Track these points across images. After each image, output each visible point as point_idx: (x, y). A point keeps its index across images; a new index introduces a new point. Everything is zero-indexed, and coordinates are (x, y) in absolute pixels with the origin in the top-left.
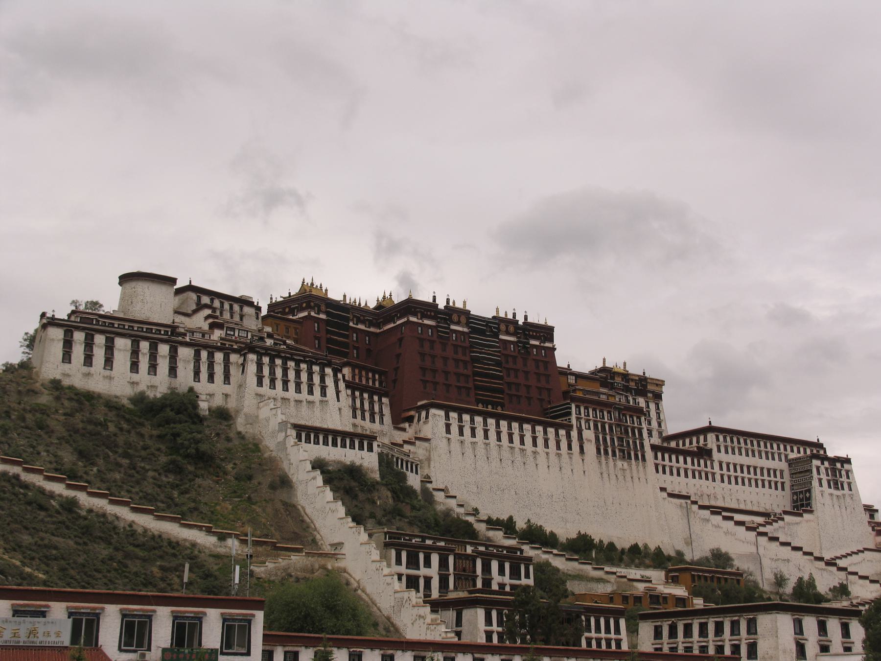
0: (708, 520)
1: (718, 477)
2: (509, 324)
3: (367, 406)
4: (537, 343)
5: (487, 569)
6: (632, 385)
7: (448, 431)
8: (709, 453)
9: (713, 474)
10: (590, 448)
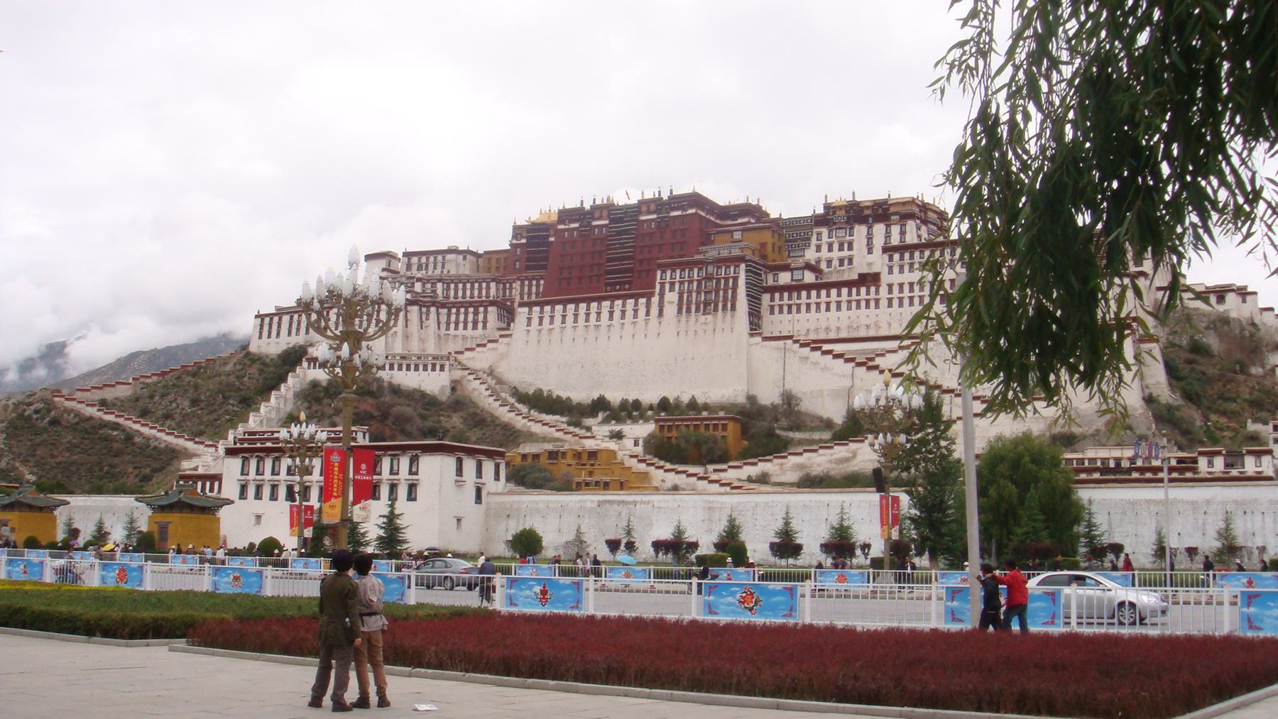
1: (884, 303)
2: (657, 205)
3: (471, 317)
6: (867, 212)
7: (529, 324)
9: (877, 301)
10: (670, 310)
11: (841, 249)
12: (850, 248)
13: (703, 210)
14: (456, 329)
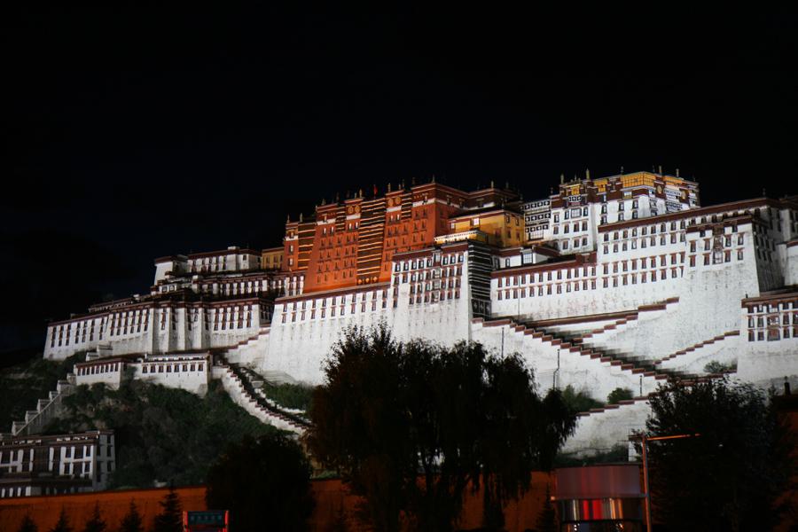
0: (522, 342)
1: (600, 282)
3: (236, 317)
4: (420, 204)
5: (57, 455)
6: (602, 191)
8: (592, 259)
11: (576, 229)
12: (585, 228)
13: (445, 199)
14: (223, 328)
